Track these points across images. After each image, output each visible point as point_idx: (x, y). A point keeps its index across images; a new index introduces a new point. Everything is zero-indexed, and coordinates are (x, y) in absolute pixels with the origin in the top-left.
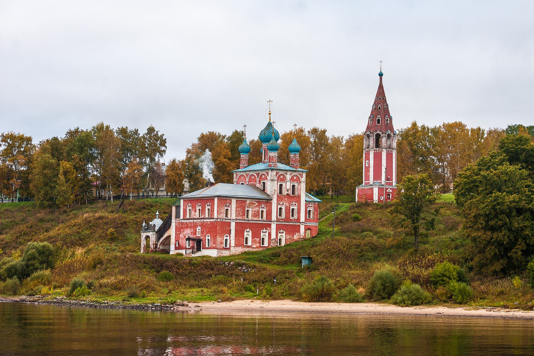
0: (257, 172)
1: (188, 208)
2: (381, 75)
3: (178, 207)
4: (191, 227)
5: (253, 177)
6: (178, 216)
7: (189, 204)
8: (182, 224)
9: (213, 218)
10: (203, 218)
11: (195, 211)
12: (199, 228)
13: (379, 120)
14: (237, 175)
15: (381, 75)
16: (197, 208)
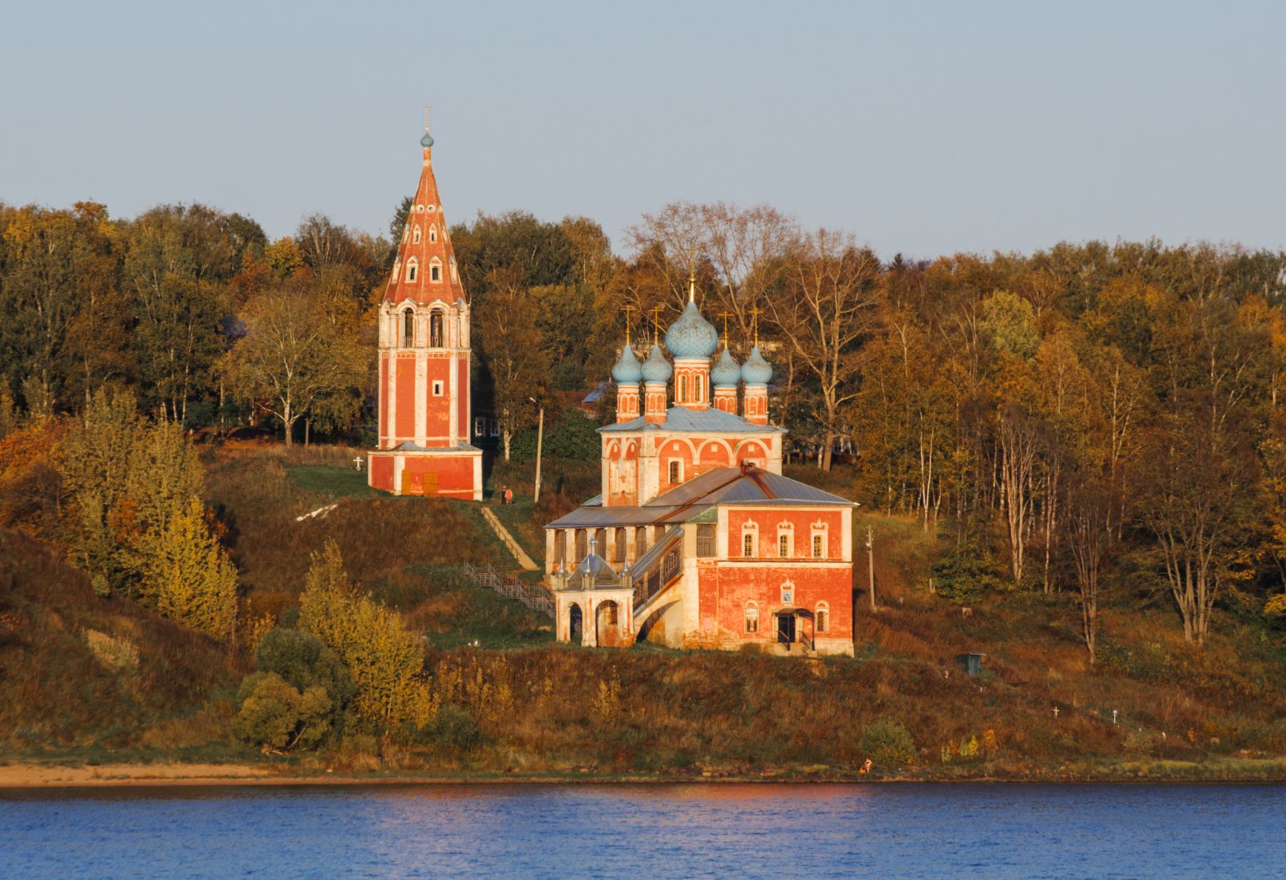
0: (731, 436)
1: (745, 532)
2: (428, 142)
3: (707, 529)
4: (758, 581)
5: (714, 448)
6: (705, 548)
7: (750, 523)
8: (727, 572)
9: (840, 561)
10: (804, 561)
11: (774, 540)
12: (788, 583)
13: (435, 270)
14: (658, 441)
15: (428, 142)
16: (781, 533)
